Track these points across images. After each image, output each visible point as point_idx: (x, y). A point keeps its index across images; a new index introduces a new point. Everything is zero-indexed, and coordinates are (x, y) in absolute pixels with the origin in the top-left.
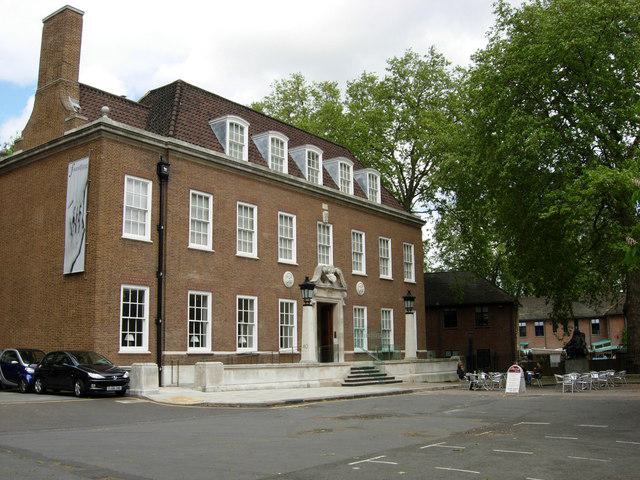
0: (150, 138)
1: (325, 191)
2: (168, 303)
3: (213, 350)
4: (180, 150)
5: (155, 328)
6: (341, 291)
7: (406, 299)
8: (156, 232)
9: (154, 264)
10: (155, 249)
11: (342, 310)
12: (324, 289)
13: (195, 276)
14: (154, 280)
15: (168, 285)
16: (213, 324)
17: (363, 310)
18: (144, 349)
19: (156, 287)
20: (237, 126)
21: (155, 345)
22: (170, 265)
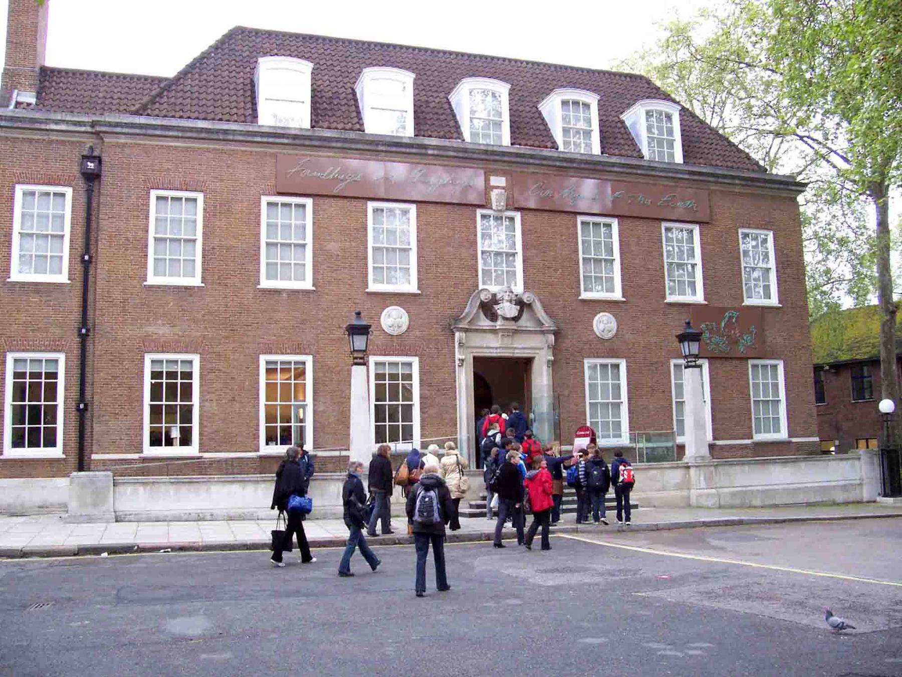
0: (57, 122)
1: (517, 155)
2: (98, 377)
3: (201, 451)
4: (119, 130)
5: (74, 416)
6: (543, 332)
7: (682, 338)
8: (79, 267)
9: (75, 316)
10: (78, 292)
11: (545, 368)
12: (494, 331)
13: (162, 331)
14: (74, 342)
15: (98, 348)
16: (201, 407)
17: (616, 367)
18: (56, 452)
19: (76, 352)
20: (576, 103)
21: (74, 444)
22: (102, 316)
